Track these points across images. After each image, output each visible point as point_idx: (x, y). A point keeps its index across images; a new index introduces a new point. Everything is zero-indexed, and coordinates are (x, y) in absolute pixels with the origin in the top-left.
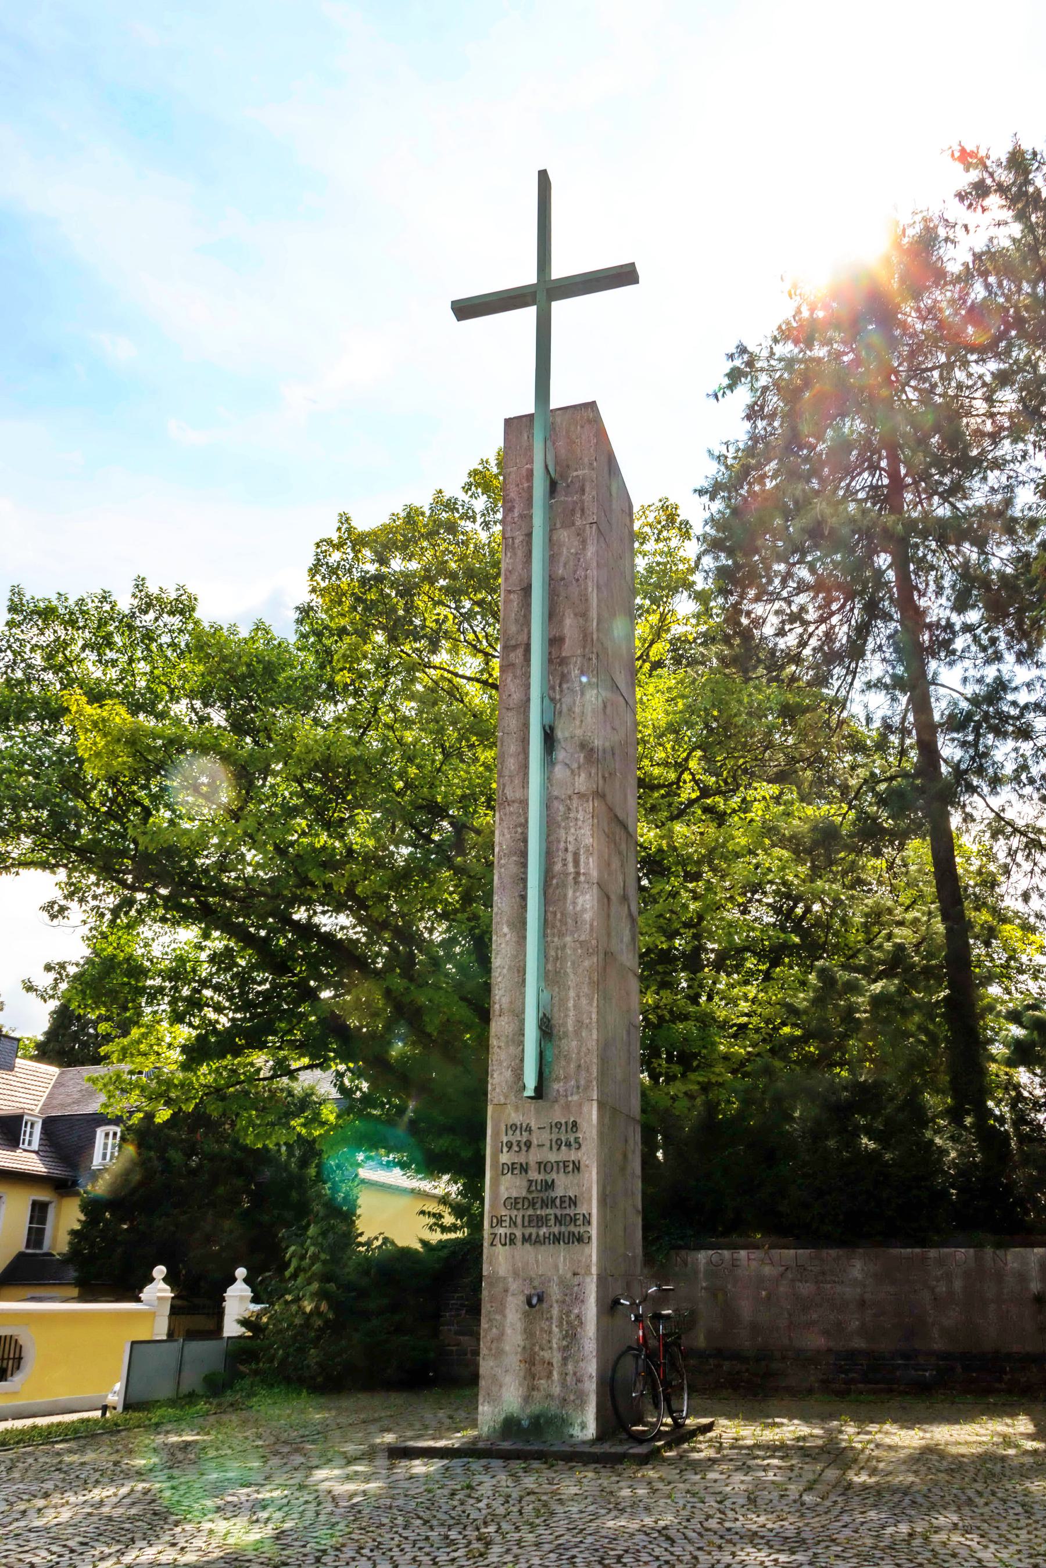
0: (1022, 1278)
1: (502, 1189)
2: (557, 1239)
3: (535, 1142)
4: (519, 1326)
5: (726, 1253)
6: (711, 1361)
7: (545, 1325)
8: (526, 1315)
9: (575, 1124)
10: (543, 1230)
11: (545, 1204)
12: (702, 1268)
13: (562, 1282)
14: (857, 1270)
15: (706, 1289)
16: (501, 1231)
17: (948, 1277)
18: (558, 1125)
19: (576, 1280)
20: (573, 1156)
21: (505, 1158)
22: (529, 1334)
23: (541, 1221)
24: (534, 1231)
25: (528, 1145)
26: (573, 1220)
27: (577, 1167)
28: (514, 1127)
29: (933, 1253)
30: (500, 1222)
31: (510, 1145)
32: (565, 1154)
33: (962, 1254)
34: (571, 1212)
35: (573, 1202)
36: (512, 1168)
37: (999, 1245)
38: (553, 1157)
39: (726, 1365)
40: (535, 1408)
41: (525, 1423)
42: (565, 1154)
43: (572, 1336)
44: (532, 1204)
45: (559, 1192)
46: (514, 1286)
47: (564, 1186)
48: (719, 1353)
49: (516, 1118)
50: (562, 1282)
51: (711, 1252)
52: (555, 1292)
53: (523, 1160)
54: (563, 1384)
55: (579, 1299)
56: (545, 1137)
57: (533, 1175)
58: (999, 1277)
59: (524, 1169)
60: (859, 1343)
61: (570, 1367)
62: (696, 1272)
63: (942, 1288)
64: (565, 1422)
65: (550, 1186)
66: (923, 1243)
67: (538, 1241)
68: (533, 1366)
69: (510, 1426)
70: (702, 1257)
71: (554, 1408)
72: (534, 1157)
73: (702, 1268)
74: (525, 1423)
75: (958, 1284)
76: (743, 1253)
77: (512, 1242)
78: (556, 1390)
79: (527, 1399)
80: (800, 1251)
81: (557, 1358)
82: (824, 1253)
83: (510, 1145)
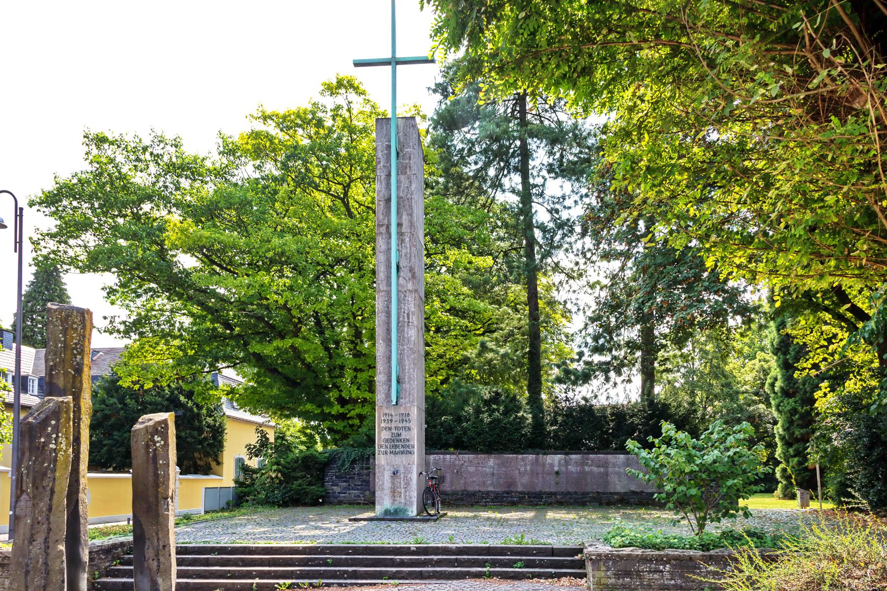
0: (552, 465)
2: (402, 453)
11: (398, 441)
12: (432, 461)
14: (491, 462)
17: (525, 465)
21: (383, 425)
22: (393, 483)
25: (391, 421)
27: (409, 429)
29: (520, 456)
30: (381, 446)
31: (384, 420)
32: (405, 424)
33: (531, 457)
36: (386, 428)
37: (545, 454)
38: (400, 425)
42: (405, 424)
43: (408, 484)
45: (403, 437)
46: (387, 468)
47: (404, 435)
49: (386, 411)
50: (404, 467)
52: (402, 470)
55: (410, 472)
56: (398, 418)
57: (393, 431)
58: (544, 465)
59: (390, 429)
60: (491, 489)
63: (522, 469)
65: (399, 435)
67: (396, 453)
72: (393, 425)
73: (432, 461)
75: (528, 468)
76: (448, 456)
83: (384, 420)
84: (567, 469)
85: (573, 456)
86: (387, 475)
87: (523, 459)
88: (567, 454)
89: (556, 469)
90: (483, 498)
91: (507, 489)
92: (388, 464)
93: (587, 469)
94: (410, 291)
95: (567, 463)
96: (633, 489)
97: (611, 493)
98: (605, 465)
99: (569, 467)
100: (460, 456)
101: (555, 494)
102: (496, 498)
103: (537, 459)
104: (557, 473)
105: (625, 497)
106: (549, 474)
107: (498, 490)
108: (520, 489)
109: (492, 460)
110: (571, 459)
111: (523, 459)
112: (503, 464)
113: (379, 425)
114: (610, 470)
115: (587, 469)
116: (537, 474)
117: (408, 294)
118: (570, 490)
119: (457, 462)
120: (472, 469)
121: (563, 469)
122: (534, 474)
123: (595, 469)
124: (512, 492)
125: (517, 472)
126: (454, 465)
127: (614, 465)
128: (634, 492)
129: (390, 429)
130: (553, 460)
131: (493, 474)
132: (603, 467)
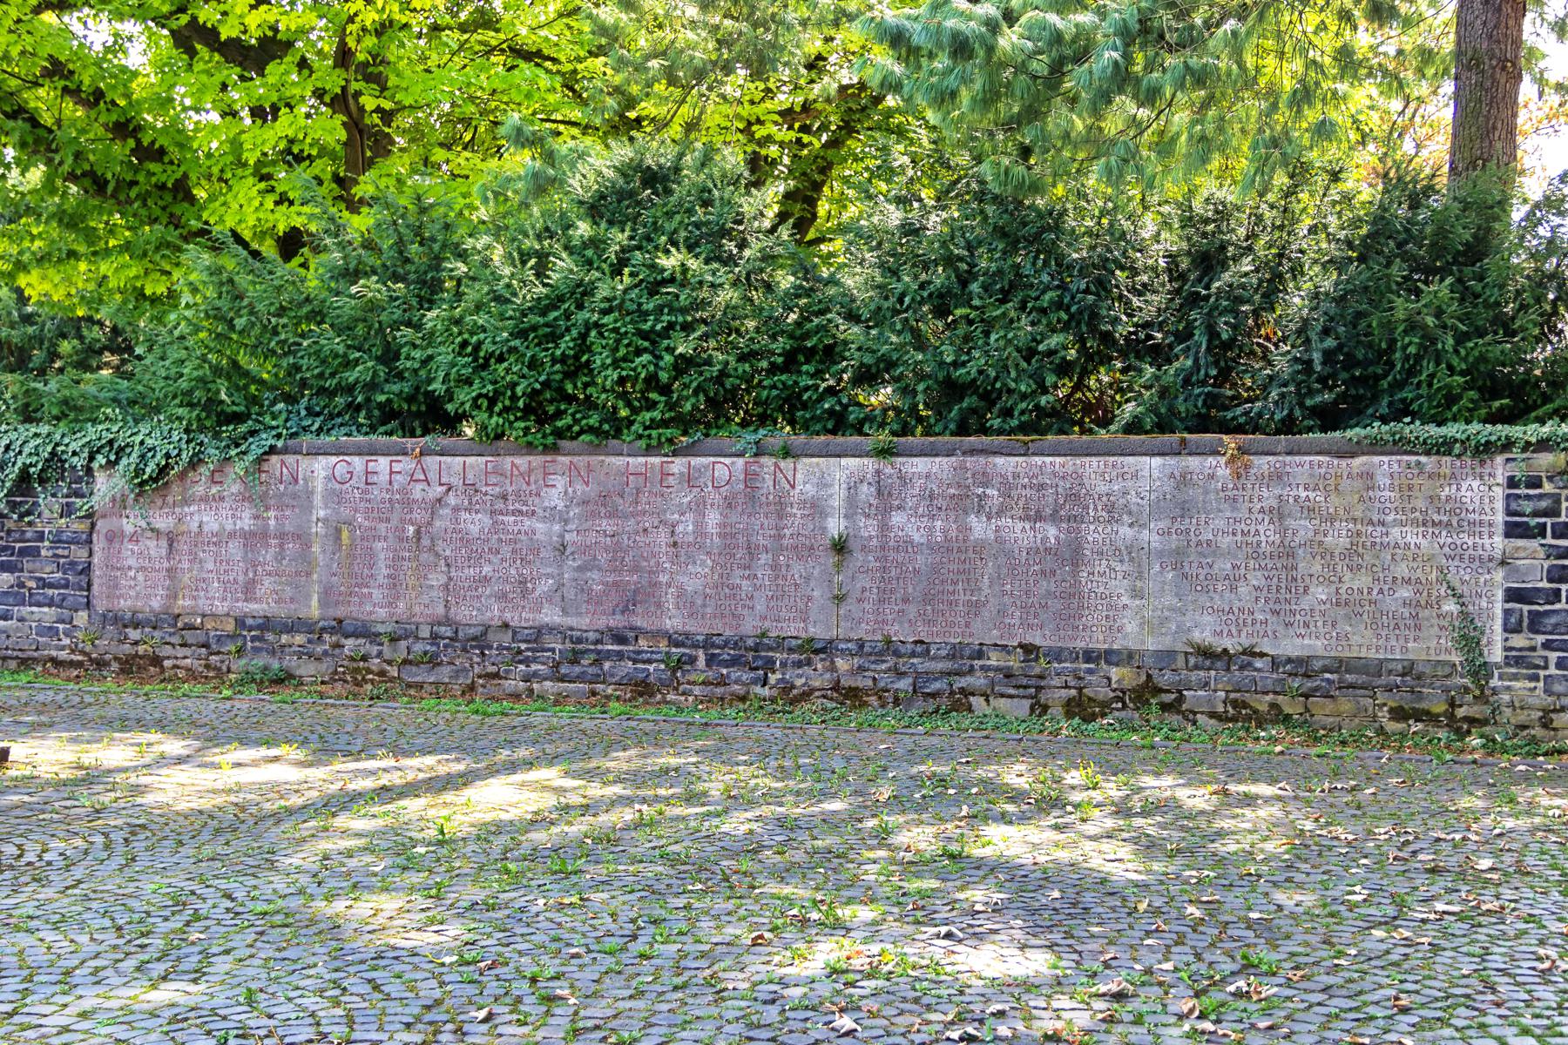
5: (358, 462)
6: (326, 637)
12: (319, 486)
14: (557, 489)
15: (325, 521)
17: (699, 507)
29: (678, 465)
39: (349, 643)
48: (339, 627)
51: (334, 459)
60: (551, 616)
62: (310, 494)
63: (687, 527)
70: (320, 467)
73: (319, 486)
75: (713, 519)
76: (383, 462)
80: (470, 460)
84: (884, 527)
85: (919, 465)
89: (835, 526)
90: (518, 657)
91: (617, 621)
93: (980, 528)
96: (1204, 635)
97: (1089, 656)
98: (1070, 507)
99: (897, 519)
100: (431, 462)
101: (826, 649)
103: (750, 477)
104: (840, 547)
105: (1165, 679)
106: (804, 551)
107: (584, 622)
109: (560, 482)
111: (689, 479)
112: (602, 504)
114: (1093, 534)
115: (980, 528)
116: (752, 551)
118: (902, 633)
119: (417, 491)
120: (476, 523)
121: (868, 528)
122: (736, 550)
123: (1019, 532)
124: (639, 632)
125: (663, 537)
126: (408, 503)
127: (1113, 512)
128: (1208, 655)
130: (823, 484)
132: (1055, 518)
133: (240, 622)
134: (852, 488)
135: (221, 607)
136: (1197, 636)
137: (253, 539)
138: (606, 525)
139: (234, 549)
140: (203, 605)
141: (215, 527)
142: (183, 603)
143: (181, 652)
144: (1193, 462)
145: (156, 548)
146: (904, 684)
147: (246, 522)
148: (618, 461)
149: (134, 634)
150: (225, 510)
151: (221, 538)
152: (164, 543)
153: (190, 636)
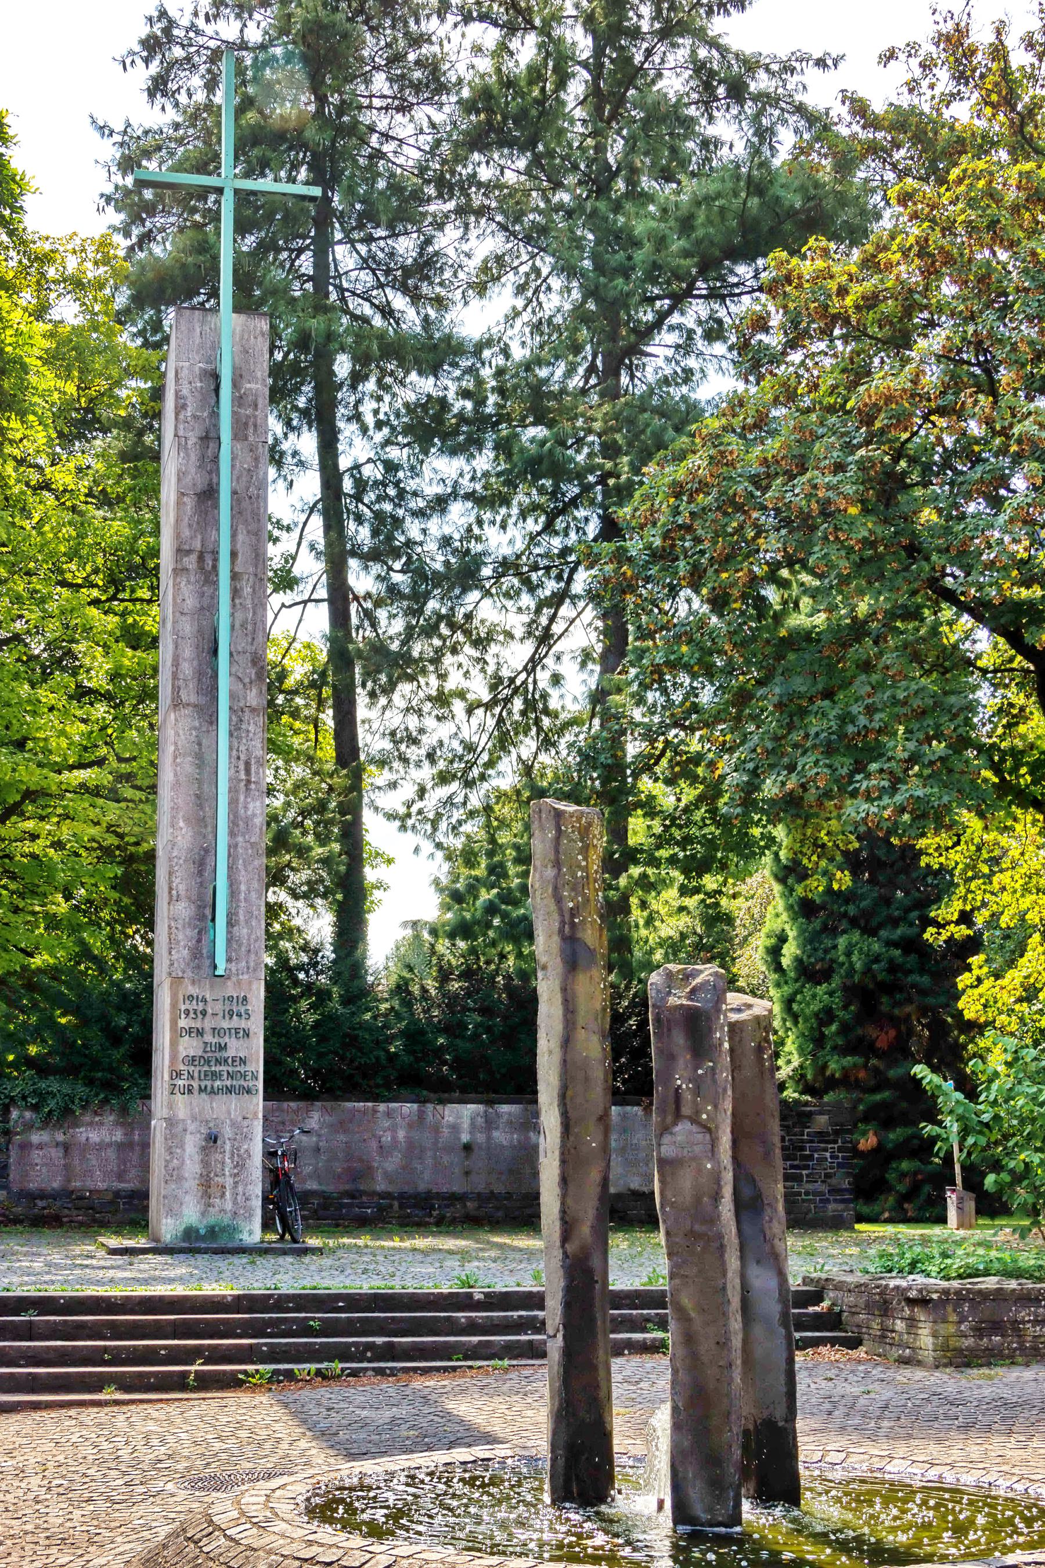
0: (455, 1128)
1: (181, 1048)
2: (229, 1090)
3: (210, 1011)
4: (197, 1158)
7: (219, 1157)
8: (204, 1149)
9: (245, 999)
10: (218, 1083)
11: (218, 1062)
13: (233, 1124)
16: (181, 1082)
17: (393, 1129)
18: (231, 998)
19: (246, 1123)
20: (243, 1024)
21: (183, 1023)
22: (205, 1163)
23: (215, 1076)
24: (209, 1083)
25: (204, 1013)
26: (244, 1076)
27: (247, 1034)
28: (191, 997)
29: (382, 1107)
30: (179, 1075)
31: (187, 1012)
32: (235, 1022)
33: (409, 1108)
34: (242, 1069)
35: (243, 1061)
36: (190, 1031)
37: (442, 1102)
38: (225, 1024)
40: (212, 1220)
41: (202, 1232)
42: (235, 1022)
43: (240, 1166)
44: (208, 1062)
45: (231, 1053)
46: (192, 1127)
47: (235, 1048)
49: (193, 990)
50: (233, 1124)
52: (227, 1132)
53: (199, 1025)
54: (235, 1202)
55: (247, 1137)
56: (219, 1007)
57: (208, 1038)
58: (436, 1129)
59: (200, 1033)
61: (240, 1189)
63: (387, 1138)
64: (236, 1229)
65: (223, 1048)
66: (377, 1098)
68: (207, 1187)
69: (189, 1233)
71: (226, 1220)
72: (208, 1024)
74: (202, 1232)
75: (401, 1134)
77: (190, 1091)
78: (229, 1206)
79: (203, 1214)
81: (229, 1182)
82: (285, 1104)
83: (187, 1012)
84: (489, 1138)
85: (505, 1108)
86: (192, 1145)
87: (389, 1114)
88: (490, 1103)
89: (465, 1138)
91: (347, 1187)
92: (194, 1119)
94: (253, 710)
95: (490, 1124)
99: (496, 1134)
102: (325, 1207)
103: (421, 1115)
104: (467, 1148)
105: (619, 1206)
106: (449, 1149)
107: (329, 1188)
108: (381, 1186)
109: (316, 1115)
110: (498, 1115)
111: (389, 1114)
112: (341, 1126)
113: (174, 1023)
116: (423, 1150)
117: (247, 716)
118: (499, 1188)
121: (481, 1138)
122: (412, 1149)
124: (362, 1193)
125: (374, 1145)
129: (200, 1033)
130: (459, 1117)
131: (318, 1149)
133: (117, 1194)
134: (473, 1119)
135: (101, 1186)
136: (632, 1186)
137: (120, 1147)
138: (342, 1137)
139: (111, 1154)
140: (90, 1184)
141: (97, 1140)
142: (76, 1184)
143: (75, 1212)
144: (628, 1108)
145: (56, 1154)
146: (500, 1214)
147: (118, 1136)
148: (349, 1105)
149: (40, 1203)
150: (104, 1132)
151: (101, 1147)
152: (61, 1150)
153: (80, 1203)
